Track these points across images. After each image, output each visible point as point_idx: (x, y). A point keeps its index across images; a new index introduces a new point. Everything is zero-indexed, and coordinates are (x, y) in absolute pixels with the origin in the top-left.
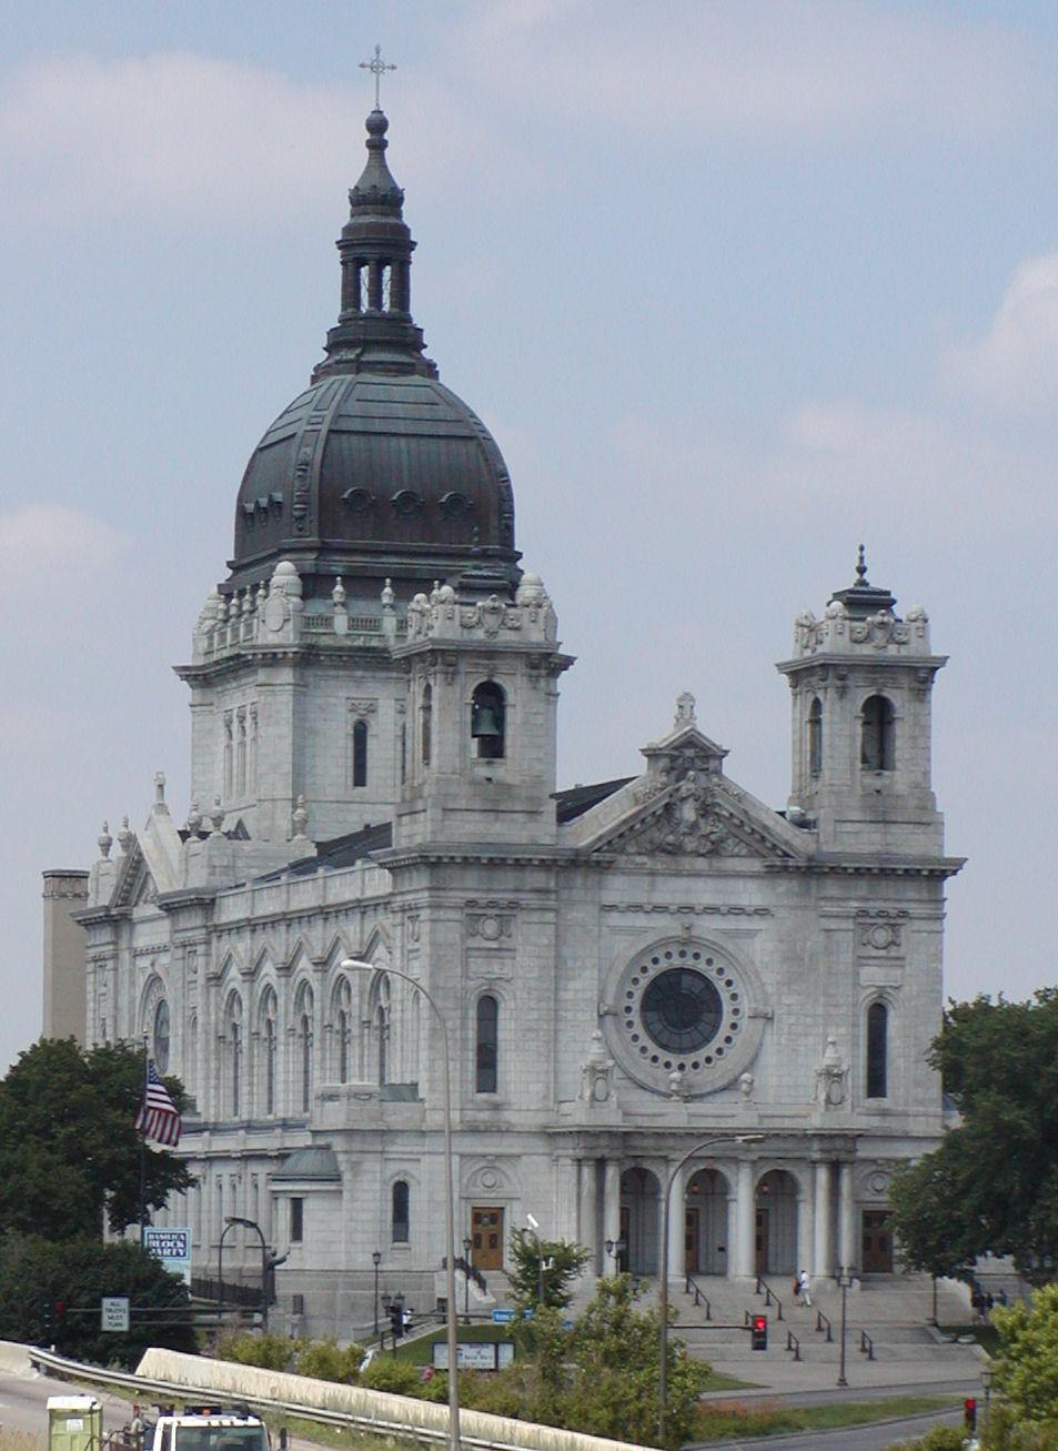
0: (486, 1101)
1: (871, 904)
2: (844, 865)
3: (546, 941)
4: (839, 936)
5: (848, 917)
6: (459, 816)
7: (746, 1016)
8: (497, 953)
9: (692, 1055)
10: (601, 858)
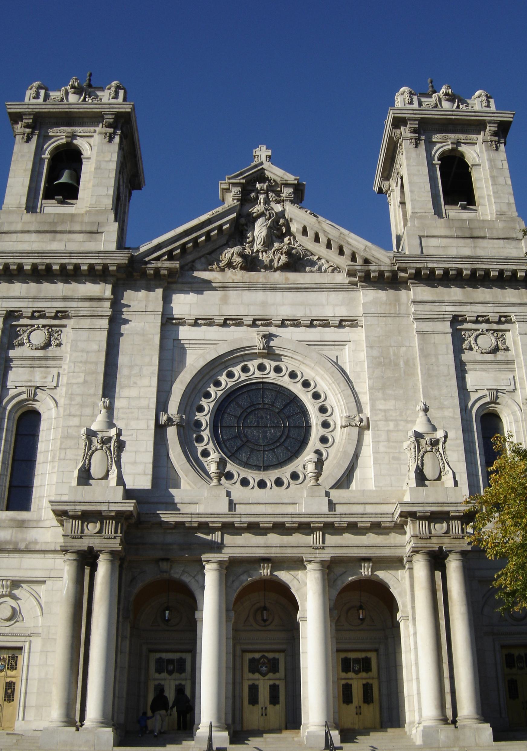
0: (13, 520)
1: (468, 308)
2: (430, 265)
3: (95, 347)
4: (437, 338)
5: (444, 320)
6: (15, 235)
7: (338, 426)
8: (43, 362)
9: (276, 471)
10: (159, 265)
